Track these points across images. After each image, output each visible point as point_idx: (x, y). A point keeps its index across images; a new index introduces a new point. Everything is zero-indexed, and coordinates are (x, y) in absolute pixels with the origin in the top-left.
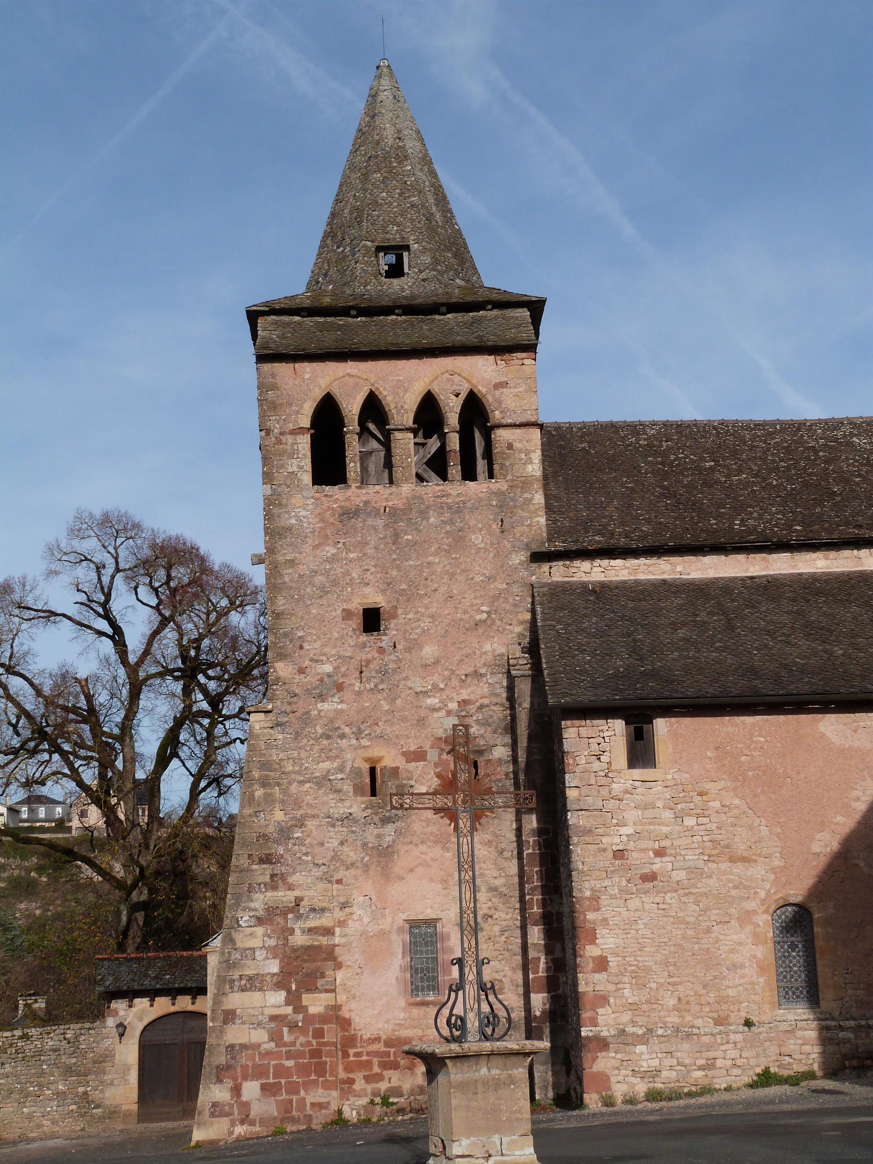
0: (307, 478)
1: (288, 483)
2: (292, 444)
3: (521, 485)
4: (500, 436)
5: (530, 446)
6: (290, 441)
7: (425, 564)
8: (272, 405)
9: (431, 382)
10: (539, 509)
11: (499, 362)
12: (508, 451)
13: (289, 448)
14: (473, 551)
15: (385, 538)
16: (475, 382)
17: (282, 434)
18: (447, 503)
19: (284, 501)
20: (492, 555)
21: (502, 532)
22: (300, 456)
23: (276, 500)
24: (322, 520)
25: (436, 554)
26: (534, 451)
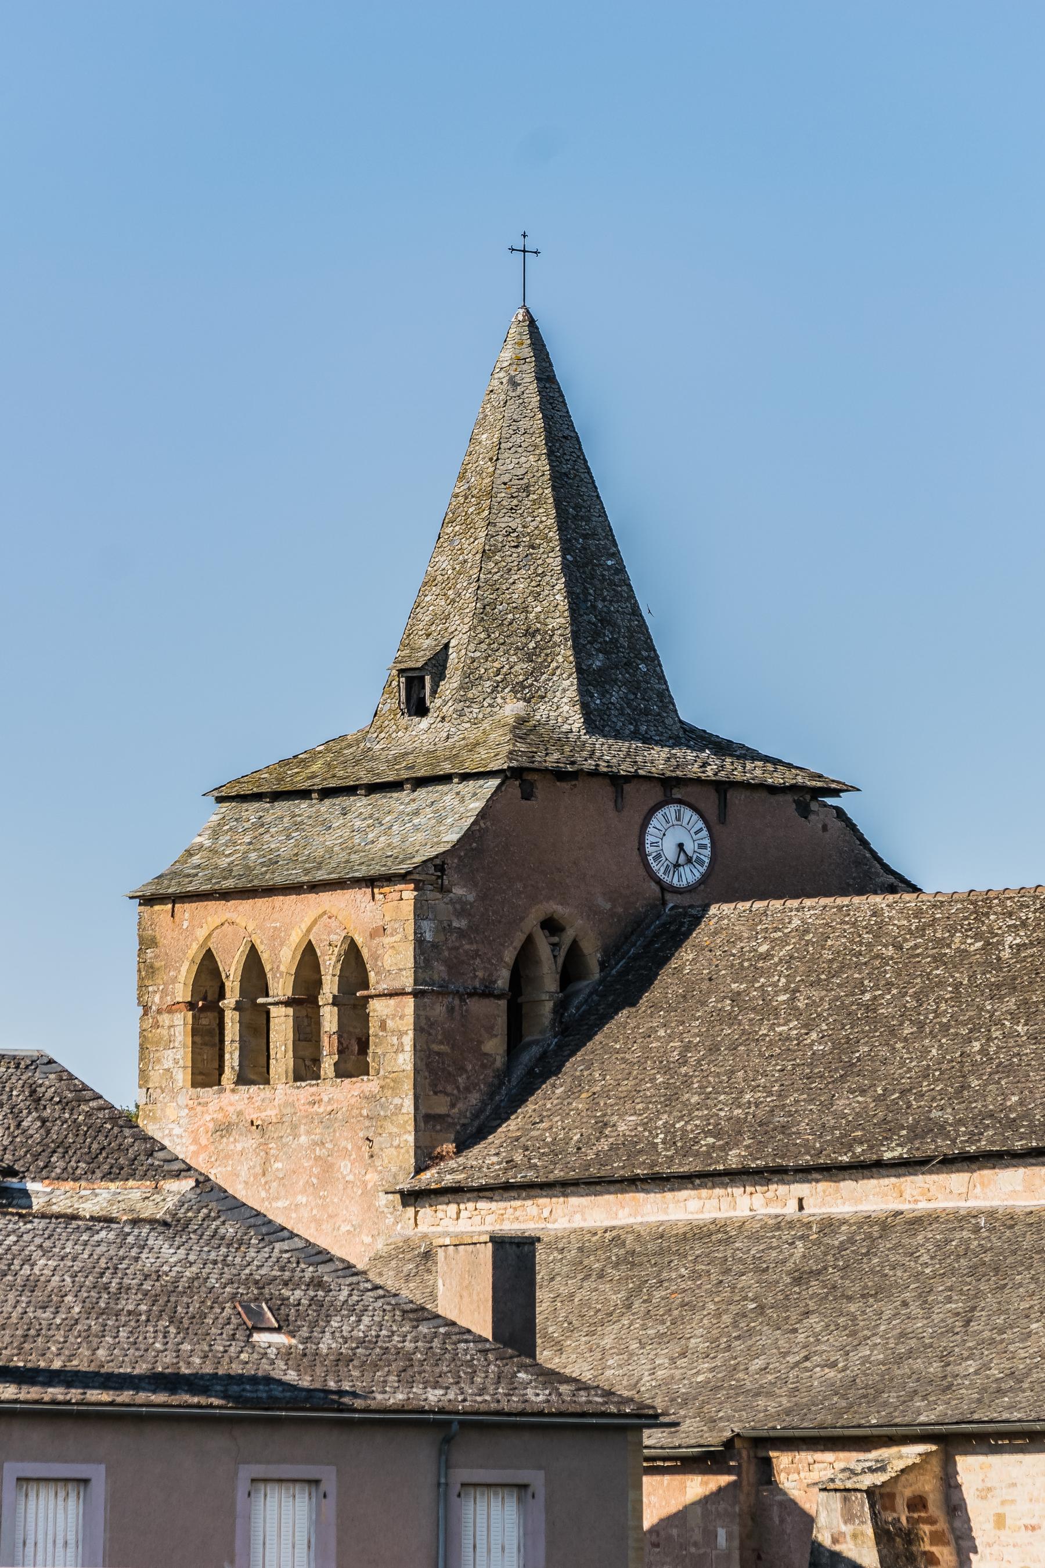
0: (182, 1077)
1: (163, 1086)
2: (170, 1027)
3: (392, 1084)
4: (374, 1011)
5: (402, 1025)
6: (167, 1023)
7: (293, 1207)
8: (151, 970)
9: (309, 930)
10: (407, 1121)
11: (378, 897)
12: (381, 1034)
13: (165, 1032)
14: (341, 1187)
15: (255, 1166)
16: (351, 927)
17: (159, 1012)
18: (317, 1114)
19: (159, 1113)
20: (360, 1192)
21: (372, 1156)
22: (176, 1044)
23: (150, 1111)
24: (195, 1141)
25: (304, 1192)
26: (406, 1033)
